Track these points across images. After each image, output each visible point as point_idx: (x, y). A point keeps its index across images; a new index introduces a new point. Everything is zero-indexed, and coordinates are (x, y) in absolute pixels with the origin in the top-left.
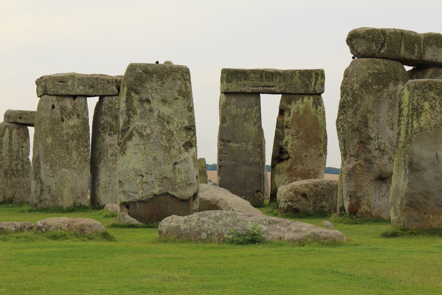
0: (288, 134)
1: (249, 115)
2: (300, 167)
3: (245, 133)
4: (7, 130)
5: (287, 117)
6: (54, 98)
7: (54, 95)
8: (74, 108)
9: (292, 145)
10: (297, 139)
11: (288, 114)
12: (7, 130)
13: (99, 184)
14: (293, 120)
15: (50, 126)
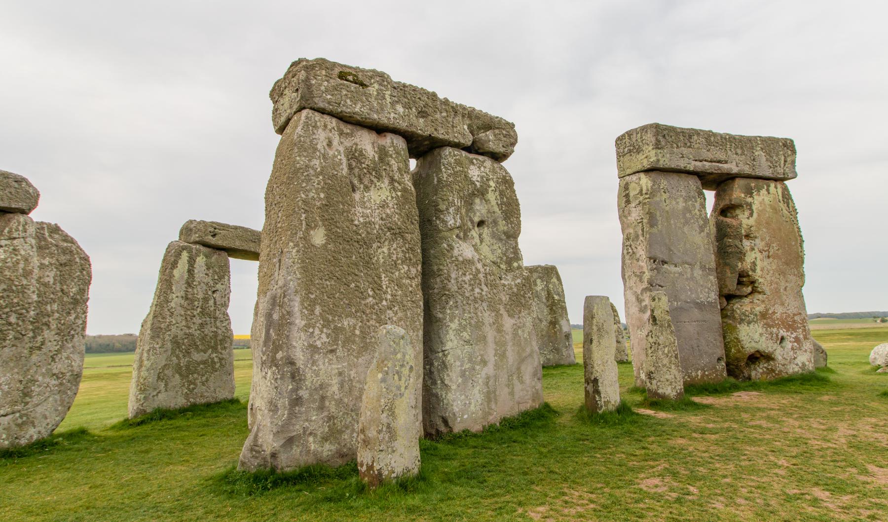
0: (752, 249)
1: (690, 212)
2: (779, 310)
3: (688, 246)
4: (185, 255)
5: (748, 218)
6: (333, 123)
7: (331, 114)
8: (381, 159)
9: (762, 270)
10: (769, 257)
11: (747, 213)
12: (185, 255)
13: (444, 366)
14: (758, 222)
15: (322, 195)
